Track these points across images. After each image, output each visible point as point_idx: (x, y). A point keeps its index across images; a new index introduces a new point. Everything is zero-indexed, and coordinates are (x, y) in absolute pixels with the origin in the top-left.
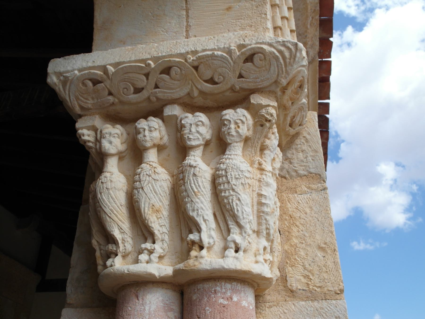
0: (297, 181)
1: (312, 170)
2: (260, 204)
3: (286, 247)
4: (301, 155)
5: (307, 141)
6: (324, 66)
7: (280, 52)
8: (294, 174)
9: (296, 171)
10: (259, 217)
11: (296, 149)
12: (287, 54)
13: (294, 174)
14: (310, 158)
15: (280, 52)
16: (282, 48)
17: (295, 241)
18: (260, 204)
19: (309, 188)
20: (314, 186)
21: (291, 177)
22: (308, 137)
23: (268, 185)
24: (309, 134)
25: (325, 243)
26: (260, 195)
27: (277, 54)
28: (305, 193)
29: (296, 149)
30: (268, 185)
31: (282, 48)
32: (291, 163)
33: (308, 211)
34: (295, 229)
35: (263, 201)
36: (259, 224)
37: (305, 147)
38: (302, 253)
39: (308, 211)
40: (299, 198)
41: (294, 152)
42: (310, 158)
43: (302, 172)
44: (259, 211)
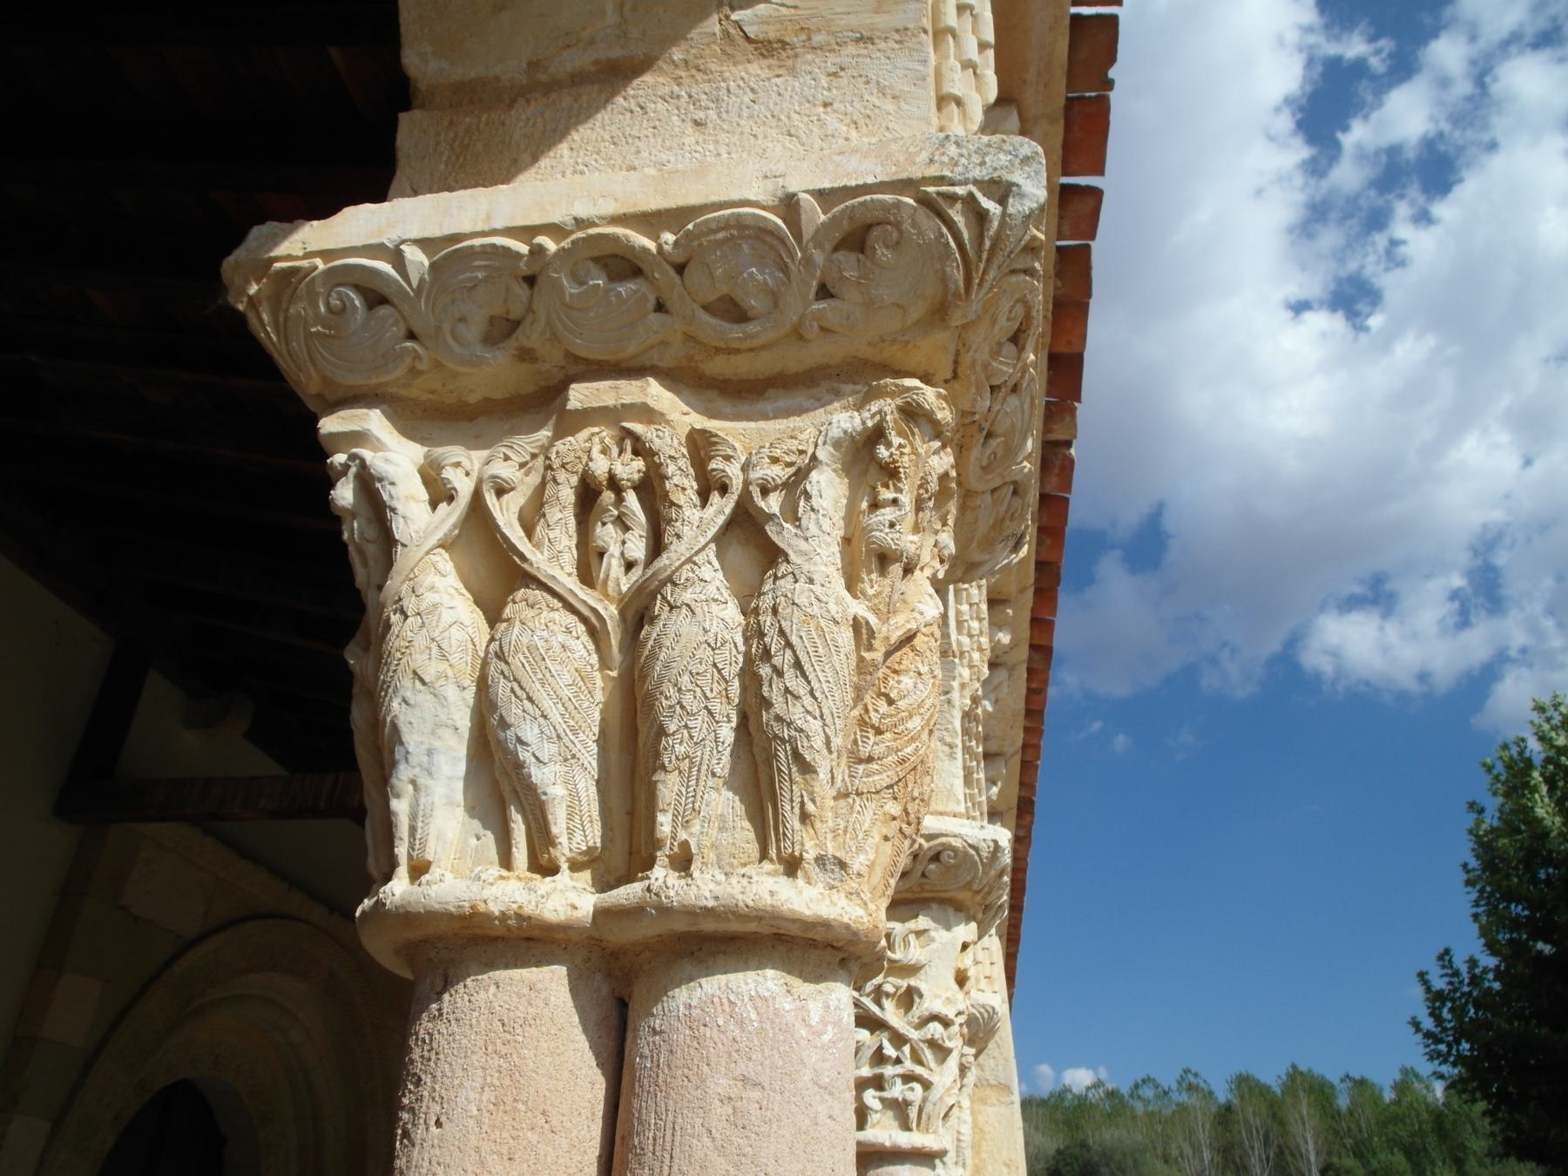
0: (988, 1091)
1: (1002, 1081)
2: (959, 1140)
3: (977, 1161)
4: (992, 1062)
5: (998, 1046)
6: (1030, 751)
7: (980, 1013)
8: (985, 1083)
9: (987, 1080)
10: (957, 1151)
11: (988, 1055)
12: (986, 1015)
13: (985, 1083)
14: (1000, 1068)
15: (980, 1013)
16: (982, 1010)
17: (984, 1156)
18: (959, 1140)
19: (998, 1100)
20: (1001, 1098)
21: (983, 1085)
22: (1000, 1042)
23: (965, 1122)
24: (1000, 1038)
25: (1010, 1160)
26: (959, 1132)
27: (978, 1015)
28: (994, 1105)
29: (988, 1055)
30: (965, 1122)
31: (982, 1010)
32: (982, 1070)
33: (996, 1125)
34: (984, 1143)
35: (962, 1138)
36: (957, 1156)
37: (996, 1054)
38: (990, 1168)
39: (996, 1125)
40: (990, 1110)
41: (986, 1057)
42: (1000, 1068)
43: (992, 1082)
44: (958, 1147)
